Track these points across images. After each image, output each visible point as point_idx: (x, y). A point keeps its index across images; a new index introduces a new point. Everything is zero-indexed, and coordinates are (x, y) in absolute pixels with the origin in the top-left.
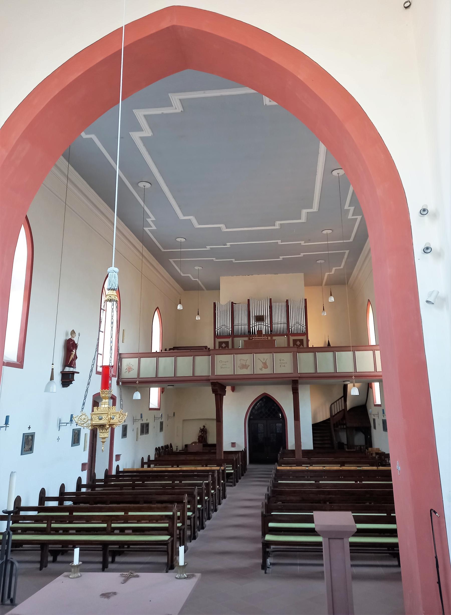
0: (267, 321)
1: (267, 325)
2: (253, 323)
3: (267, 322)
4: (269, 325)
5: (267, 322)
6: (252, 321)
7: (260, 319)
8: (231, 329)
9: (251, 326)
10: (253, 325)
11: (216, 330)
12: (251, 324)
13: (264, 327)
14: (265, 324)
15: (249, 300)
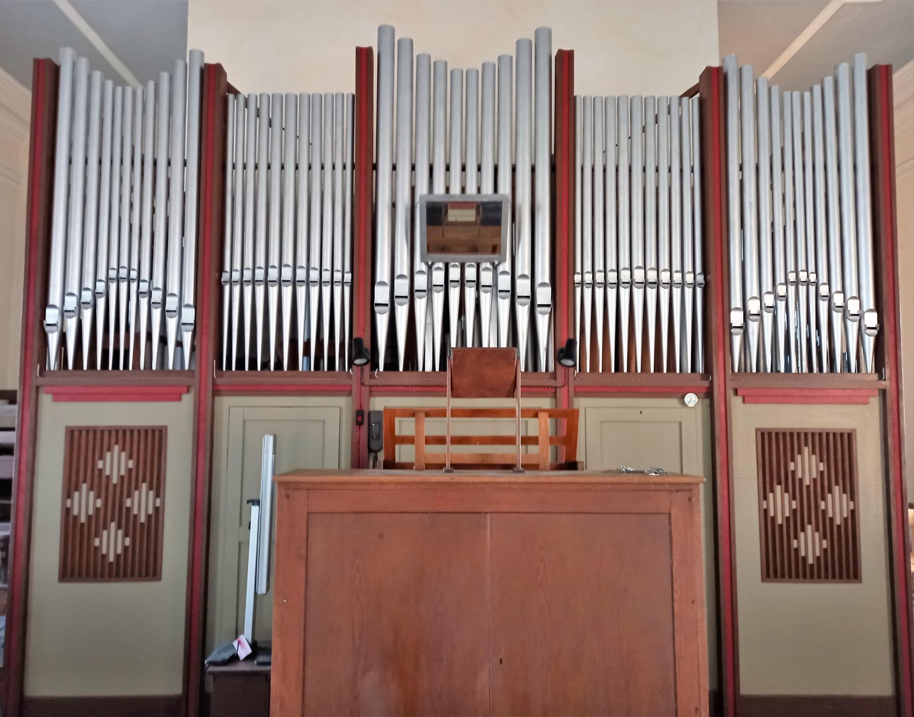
0: (529, 252)
1: (523, 288)
2: (402, 268)
3: (523, 267)
4: (544, 295)
5: (523, 267)
6: (394, 253)
7: (462, 230)
8: (189, 315)
9: (382, 295)
10: (402, 287)
11: (52, 316)
12: (383, 273)
13: (498, 305)
14: (504, 282)
15: (364, 57)
